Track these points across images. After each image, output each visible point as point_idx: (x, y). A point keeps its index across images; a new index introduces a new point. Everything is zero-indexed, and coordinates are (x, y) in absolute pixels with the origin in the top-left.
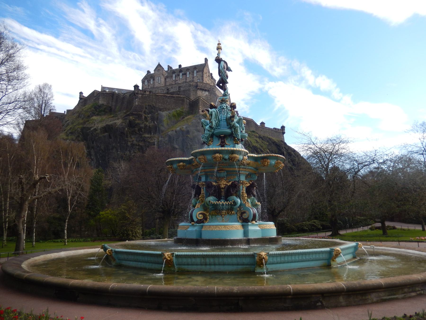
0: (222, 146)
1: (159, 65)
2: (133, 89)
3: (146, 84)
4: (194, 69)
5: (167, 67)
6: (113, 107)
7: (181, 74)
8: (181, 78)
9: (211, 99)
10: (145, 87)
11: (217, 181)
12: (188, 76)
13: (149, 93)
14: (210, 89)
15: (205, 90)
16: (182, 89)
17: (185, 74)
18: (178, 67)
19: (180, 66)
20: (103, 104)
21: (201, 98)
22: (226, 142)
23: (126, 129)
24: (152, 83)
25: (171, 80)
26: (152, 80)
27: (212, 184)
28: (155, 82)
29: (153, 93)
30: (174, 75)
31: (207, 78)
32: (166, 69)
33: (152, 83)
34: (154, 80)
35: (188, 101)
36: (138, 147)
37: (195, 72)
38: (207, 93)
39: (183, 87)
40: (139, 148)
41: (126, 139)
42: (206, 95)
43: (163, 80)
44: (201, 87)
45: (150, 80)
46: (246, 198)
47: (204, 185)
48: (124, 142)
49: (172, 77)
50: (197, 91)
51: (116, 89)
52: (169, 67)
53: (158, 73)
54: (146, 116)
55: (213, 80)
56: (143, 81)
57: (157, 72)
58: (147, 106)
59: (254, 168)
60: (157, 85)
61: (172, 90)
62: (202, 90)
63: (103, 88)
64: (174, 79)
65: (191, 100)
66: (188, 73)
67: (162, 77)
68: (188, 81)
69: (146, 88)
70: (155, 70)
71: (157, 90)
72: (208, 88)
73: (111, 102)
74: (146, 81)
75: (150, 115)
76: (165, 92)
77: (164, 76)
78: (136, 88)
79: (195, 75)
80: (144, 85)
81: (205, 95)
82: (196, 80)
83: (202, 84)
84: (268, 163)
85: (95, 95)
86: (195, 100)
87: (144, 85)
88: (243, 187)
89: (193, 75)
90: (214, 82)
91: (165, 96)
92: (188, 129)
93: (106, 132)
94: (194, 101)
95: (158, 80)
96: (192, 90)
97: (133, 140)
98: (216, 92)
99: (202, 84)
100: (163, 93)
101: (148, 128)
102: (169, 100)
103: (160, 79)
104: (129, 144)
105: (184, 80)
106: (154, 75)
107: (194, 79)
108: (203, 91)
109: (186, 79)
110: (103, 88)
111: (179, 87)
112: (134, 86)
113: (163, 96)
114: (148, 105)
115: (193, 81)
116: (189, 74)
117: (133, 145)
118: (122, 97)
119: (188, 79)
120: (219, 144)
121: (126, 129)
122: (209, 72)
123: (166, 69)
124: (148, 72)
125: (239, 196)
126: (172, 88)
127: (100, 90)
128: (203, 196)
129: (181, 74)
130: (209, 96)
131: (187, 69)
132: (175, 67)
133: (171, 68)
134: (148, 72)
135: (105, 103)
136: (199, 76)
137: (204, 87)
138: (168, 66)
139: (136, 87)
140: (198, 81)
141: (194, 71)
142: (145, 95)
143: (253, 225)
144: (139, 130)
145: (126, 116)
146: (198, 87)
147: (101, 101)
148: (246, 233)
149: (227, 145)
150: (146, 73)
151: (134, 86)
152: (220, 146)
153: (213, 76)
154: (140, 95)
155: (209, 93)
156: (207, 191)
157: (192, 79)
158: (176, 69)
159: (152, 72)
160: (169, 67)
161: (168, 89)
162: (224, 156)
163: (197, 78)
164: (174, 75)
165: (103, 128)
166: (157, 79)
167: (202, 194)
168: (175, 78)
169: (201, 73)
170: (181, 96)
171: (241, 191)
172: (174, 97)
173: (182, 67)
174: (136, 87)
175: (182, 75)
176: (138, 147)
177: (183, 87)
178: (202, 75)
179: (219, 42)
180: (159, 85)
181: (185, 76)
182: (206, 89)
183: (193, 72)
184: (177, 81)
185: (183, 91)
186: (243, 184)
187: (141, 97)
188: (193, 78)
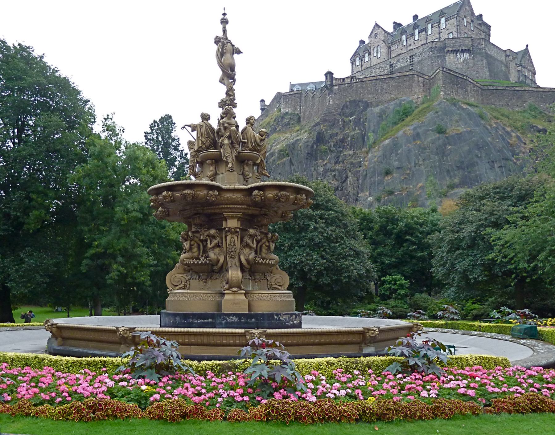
1: (377, 25)
2: (323, 79)
3: (358, 64)
4: (440, 16)
5: (392, 26)
6: (302, 115)
7: (416, 32)
8: (417, 38)
9: (474, 64)
10: (356, 70)
12: (429, 32)
13: (351, 81)
14: (472, 46)
15: (463, 51)
16: (416, 59)
17: (425, 30)
18: (410, 21)
19: (415, 17)
20: (287, 113)
21: (445, 70)
23: (315, 147)
24: (367, 60)
25: (400, 46)
26: (367, 55)
28: (372, 56)
29: (356, 79)
30: (404, 37)
31: (468, 26)
32: (390, 29)
33: (367, 60)
34: (369, 54)
35: (421, 79)
36: (334, 173)
37: (443, 20)
38: (466, 55)
39: (418, 54)
40: (335, 175)
41: (315, 163)
42: (465, 59)
43: (384, 50)
44: (453, 47)
45: (364, 56)
48: (312, 169)
49: (401, 40)
50: (444, 56)
51: (312, 83)
52: (397, 25)
53: (376, 40)
54: (347, 119)
55: (483, 28)
56: (353, 61)
57: (373, 39)
58: (348, 103)
59: (248, 205)
60: (374, 61)
61: (398, 66)
62: (456, 51)
63: (292, 86)
64: (404, 43)
65: (426, 77)
66: (429, 26)
67: (383, 45)
68: (429, 41)
69: (358, 70)
70: (370, 36)
71: (374, 71)
72: (467, 46)
73: (298, 107)
74: (358, 59)
75: (354, 117)
76: (386, 71)
77: (386, 42)
78: (328, 77)
79: (443, 26)
80: (354, 66)
81: (462, 60)
82: (444, 36)
83: (454, 42)
84: (261, 197)
85: (279, 97)
86: (433, 76)
87: (354, 66)
89: (439, 27)
90: (487, 30)
91: (379, 79)
92: (419, 130)
93: (288, 155)
94: (432, 77)
95: (377, 52)
96: (435, 57)
97: (326, 164)
98: (487, 49)
99: (454, 42)
100: (382, 73)
101: (349, 139)
102: (385, 86)
103: (379, 50)
104: (321, 169)
105: (424, 42)
106: (369, 45)
107: (441, 34)
108: (458, 54)
109: (426, 39)
110: (292, 86)
111: (410, 57)
112: (325, 75)
113: (374, 81)
114: (350, 102)
115: (440, 38)
116: (432, 27)
117: (326, 171)
118: (312, 95)
119: (429, 37)
121: (315, 147)
122: (473, 13)
123: (390, 29)
124: (362, 42)
126: (397, 61)
127: (286, 89)
129: (416, 32)
130: (471, 61)
131: (428, 19)
132: (406, 21)
133: (400, 25)
134: (362, 42)
135: (290, 111)
136: (450, 28)
137: (460, 46)
138: (395, 23)
139: (329, 75)
140: (451, 36)
141: (440, 20)
142: (343, 86)
143: (235, 293)
144: (334, 145)
145: (314, 126)
146: (446, 49)
147: (283, 108)
148: (219, 306)
150: (358, 44)
151: (325, 75)
153: (485, 19)
154: (336, 88)
155: (470, 56)
157: (437, 36)
158: (408, 25)
159: (367, 42)
160: (397, 25)
161: (391, 66)
162: (174, 193)
163: (448, 32)
164: (404, 37)
165: (281, 151)
166: (373, 51)
168: (407, 41)
169: (454, 21)
170: (408, 73)
172: (394, 78)
173: (419, 18)
174: (329, 75)
175: (419, 33)
176: (334, 173)
177: (418, 54)
178: (456, 24)
180: (379, 61)
181: (424, 33)
182: (464, 48)
183: (439, 23)
184: (410, 45)
185: (419, 62)
186: (231, 233)
187: (338, 89)
188: (440, 33)
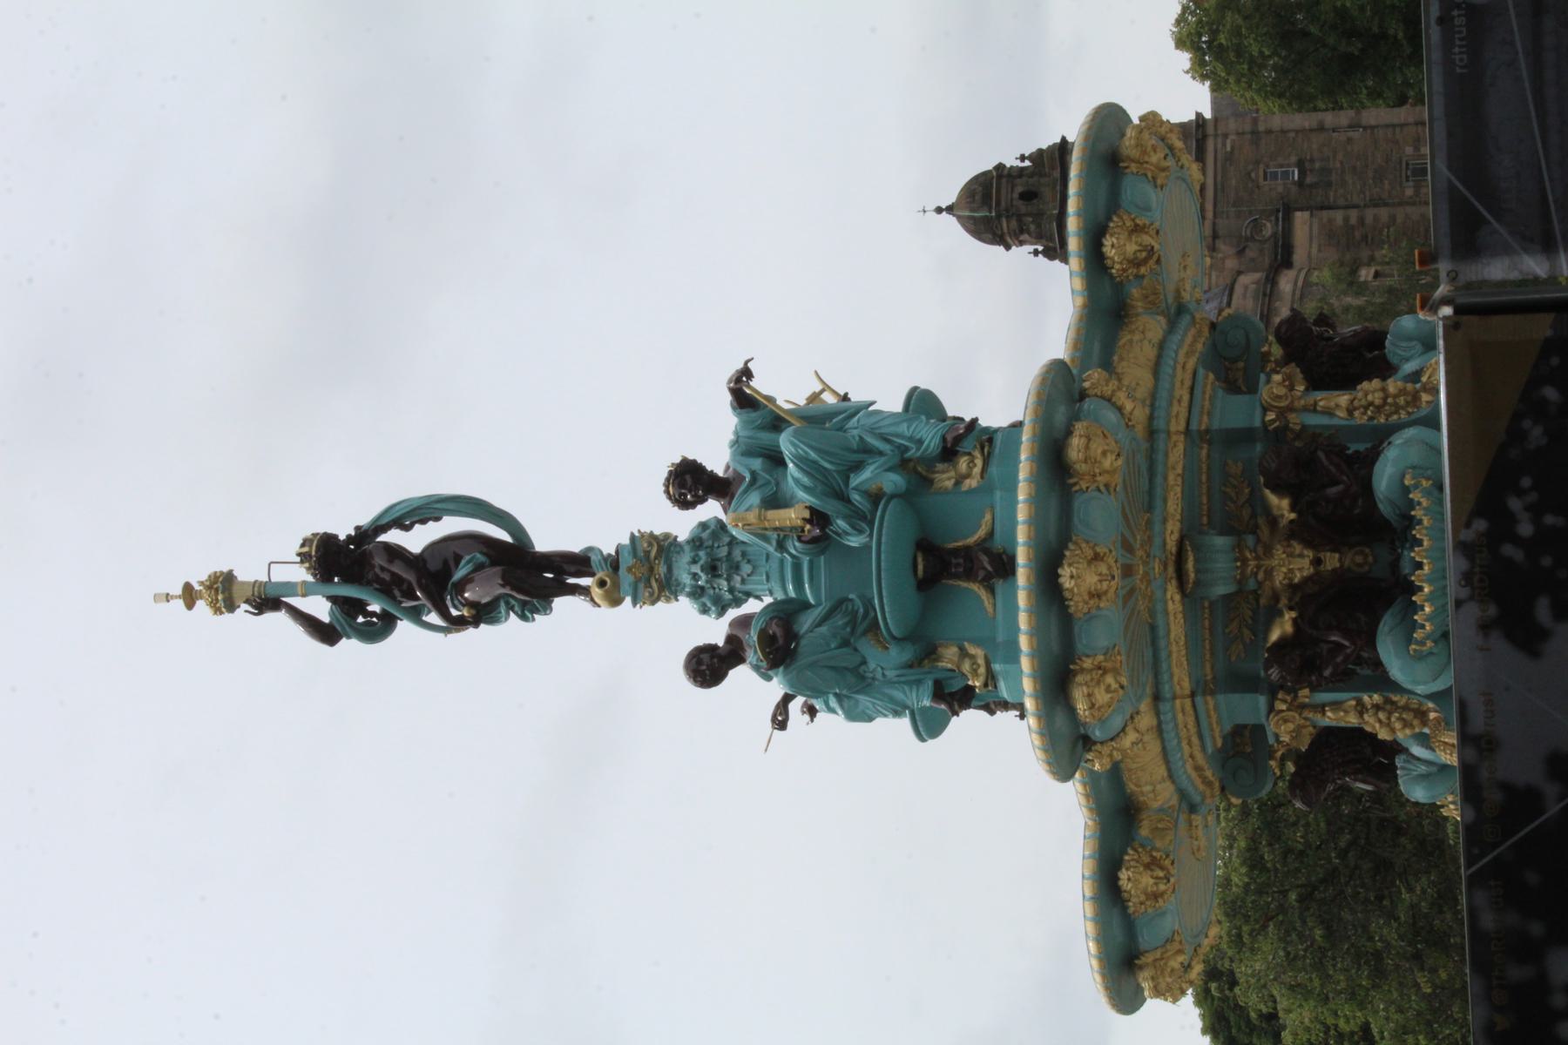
0: (1004, 566)
11: (1263, 601)
22: (971, 540)
27: (1283, 643)
46: (1393, 385)
47: (1296, 697)
88: (1313, 409)
120: (983, 594)
125: (1380, 437)
128: (1377, 707)
149: (991, 534)
152: (1000, 585)
156: (1343, 679)
167: (1361, 714)
171: (1335, 421)
179: (168, 597)
